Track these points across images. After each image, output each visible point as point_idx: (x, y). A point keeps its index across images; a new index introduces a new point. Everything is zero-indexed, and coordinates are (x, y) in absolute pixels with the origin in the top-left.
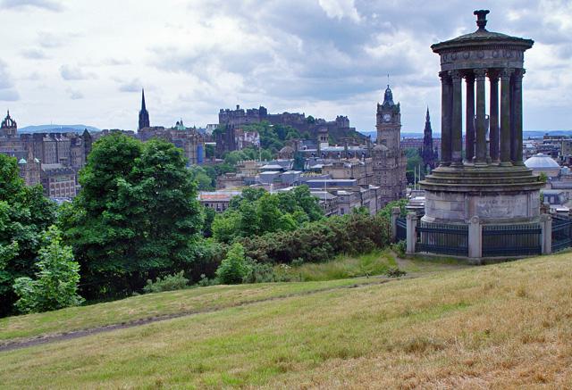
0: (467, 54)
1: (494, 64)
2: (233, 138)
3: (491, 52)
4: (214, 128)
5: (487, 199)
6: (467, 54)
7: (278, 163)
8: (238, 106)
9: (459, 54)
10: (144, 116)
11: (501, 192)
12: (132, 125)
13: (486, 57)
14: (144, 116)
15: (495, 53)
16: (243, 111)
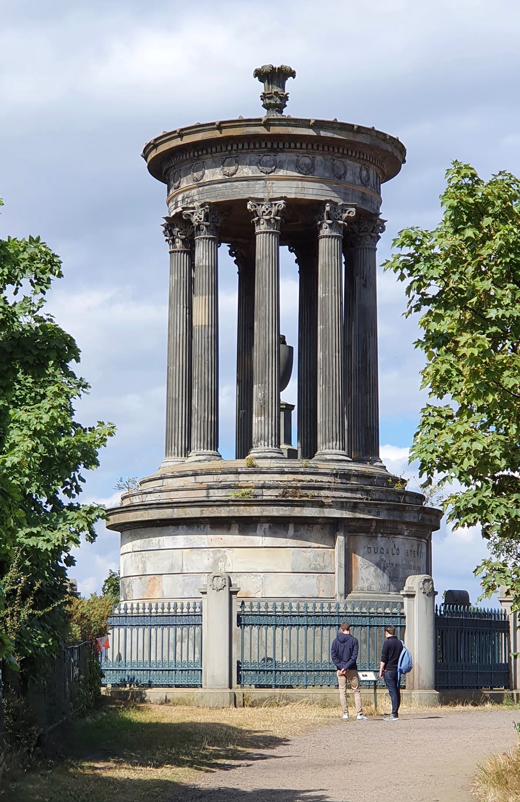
6: (307, 161)
13: (349, 177)
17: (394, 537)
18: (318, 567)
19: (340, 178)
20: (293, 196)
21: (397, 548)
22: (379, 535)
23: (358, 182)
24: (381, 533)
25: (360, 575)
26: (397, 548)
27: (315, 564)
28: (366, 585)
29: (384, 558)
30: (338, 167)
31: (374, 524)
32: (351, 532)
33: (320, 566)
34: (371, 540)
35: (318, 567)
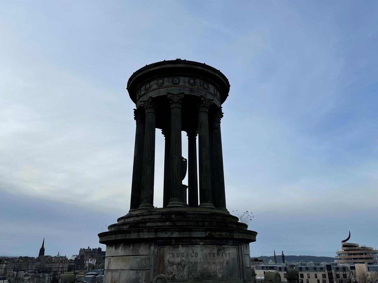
0: (161, 81)
1: (191, 90)
2: (83, 262)
3: (187, 79)
4: (75, 257)
5: (182, 250)
7: (95, 271)
8: (89, 247)
9: (152, 83)
10: (42, 250)
11: (201, 239)
12: (35, 255)
13: (181, 83)
14: (42, 250)
15: (192, 81)
16: (91, 249)
17: (192, 246)
18: (142, 266)
19: (175, 84)
20: (155, 96)
21: (195, 252)
22: (180, 246)
23: (187, 85)
24: (181, 245)
25: (167, 271)
26: (195, 252)
27: (141, 265)
28: (170, 276)
29: (185, 259)
30: (175, 80)
31: (173, 240)
32: (161, 246)
33: (143, 266)
34: (174, 249)
35: (142, 266)
